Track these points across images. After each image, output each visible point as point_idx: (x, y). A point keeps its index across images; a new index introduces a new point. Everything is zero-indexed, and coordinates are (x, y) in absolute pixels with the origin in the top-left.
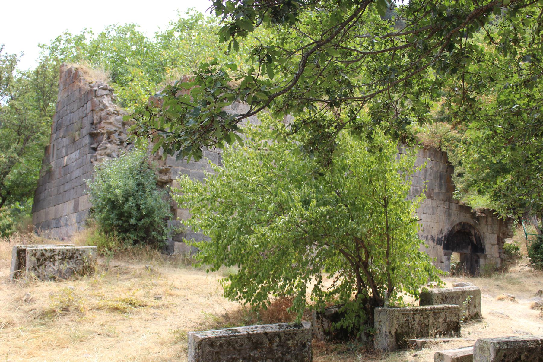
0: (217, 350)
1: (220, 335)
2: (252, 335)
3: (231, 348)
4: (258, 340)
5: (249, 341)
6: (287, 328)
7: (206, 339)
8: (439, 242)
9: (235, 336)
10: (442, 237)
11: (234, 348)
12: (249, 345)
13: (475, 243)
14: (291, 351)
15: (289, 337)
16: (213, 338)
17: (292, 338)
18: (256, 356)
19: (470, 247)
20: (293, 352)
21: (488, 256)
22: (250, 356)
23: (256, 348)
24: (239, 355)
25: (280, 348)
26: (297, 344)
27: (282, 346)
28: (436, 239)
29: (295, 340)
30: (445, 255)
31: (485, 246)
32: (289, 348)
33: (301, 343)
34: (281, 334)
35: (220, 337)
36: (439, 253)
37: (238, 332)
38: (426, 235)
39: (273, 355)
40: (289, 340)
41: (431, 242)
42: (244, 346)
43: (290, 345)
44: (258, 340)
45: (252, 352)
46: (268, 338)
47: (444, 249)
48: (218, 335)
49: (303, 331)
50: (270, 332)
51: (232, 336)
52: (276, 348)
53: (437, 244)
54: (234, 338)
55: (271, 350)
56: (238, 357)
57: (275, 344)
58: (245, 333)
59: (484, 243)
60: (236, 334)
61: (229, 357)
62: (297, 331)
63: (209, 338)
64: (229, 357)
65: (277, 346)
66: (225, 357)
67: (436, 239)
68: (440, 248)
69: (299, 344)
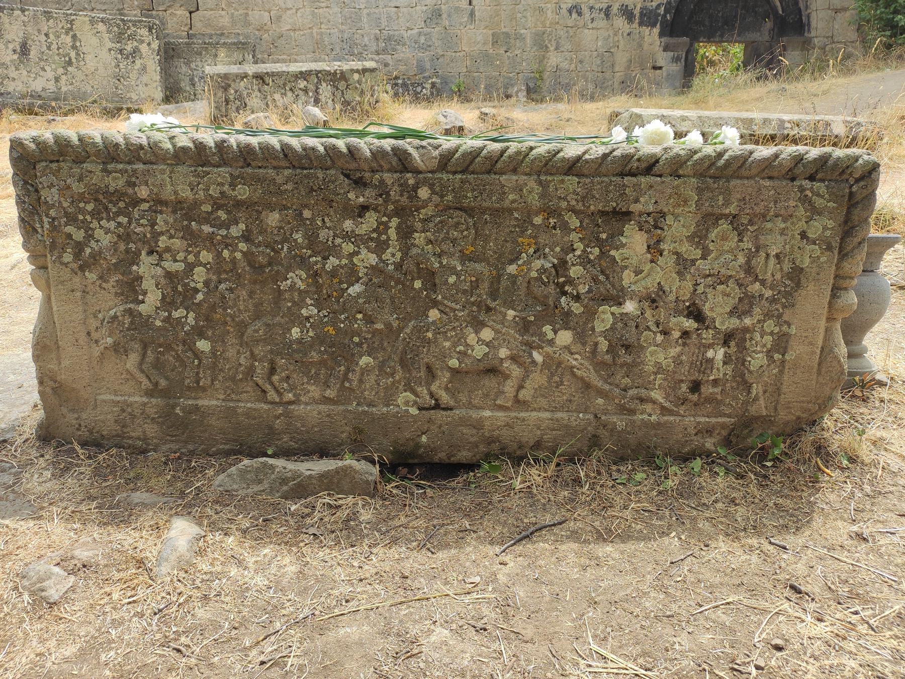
8: (648, 18)
10: (658, 6)
13: (781, 12)
19: (769, 24)
21: (816, 40)
28: (637, 12)
30: (666, 49)
31: (808, 17)
36: (646, 46)
38: (605, 6)
41: (620, 23)
47: (661, 35)
53: (641, 24)
59: (807, 7)
67: (637, 12)
68: (652, 37)
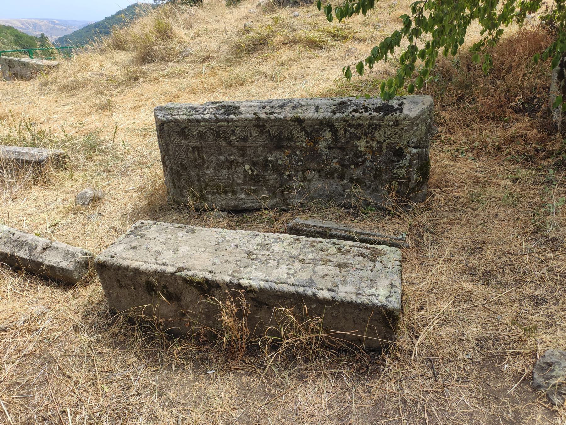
0: (194, 143)
1: (199, 117)
2: (266, 121)
3: (223, 143)
4: (280, 133)
5: (262, 133)
6: (356, 111)
7: (169, 121)
9: (227, 121)
11: (230, 143)
12: (262, 140)
14: (363, 162)
15: (359, 132)
16: (183, 121)
17: (366, 135)
18: (280, 162)
20: (367, 163)
22: (266, 160)
23: (279, 147)
24: (243, 156)
25: (335, 153)
26: (380, 149)
27: (342, 149)
29: (373, 139)
32: (358, 154)
33: (390, 147)
34: (337, 125)
35: (198, 121)
37: (235, 114)
39: (319, 163)
40: (359, 138)
42: (250, 142)
43: (362, 149)
44: (280, 133)
45: (270, 151)
46: (303, 129)
48: (194, 117)
49: (397, 123)
50: (309, 119)
51: (222, 121)
52: (326, 151)
54: (226, 123)
55: (314, 155)
56: (240, 160)
57: (322, 144)
58: (250, 116)
60: (232, 116)
61: (222, 158)
62: (381, 119)
63: (176, 120)
64: (222, 158)
65: (329, 148)
66: (213, 158)
69: (384, 150)
